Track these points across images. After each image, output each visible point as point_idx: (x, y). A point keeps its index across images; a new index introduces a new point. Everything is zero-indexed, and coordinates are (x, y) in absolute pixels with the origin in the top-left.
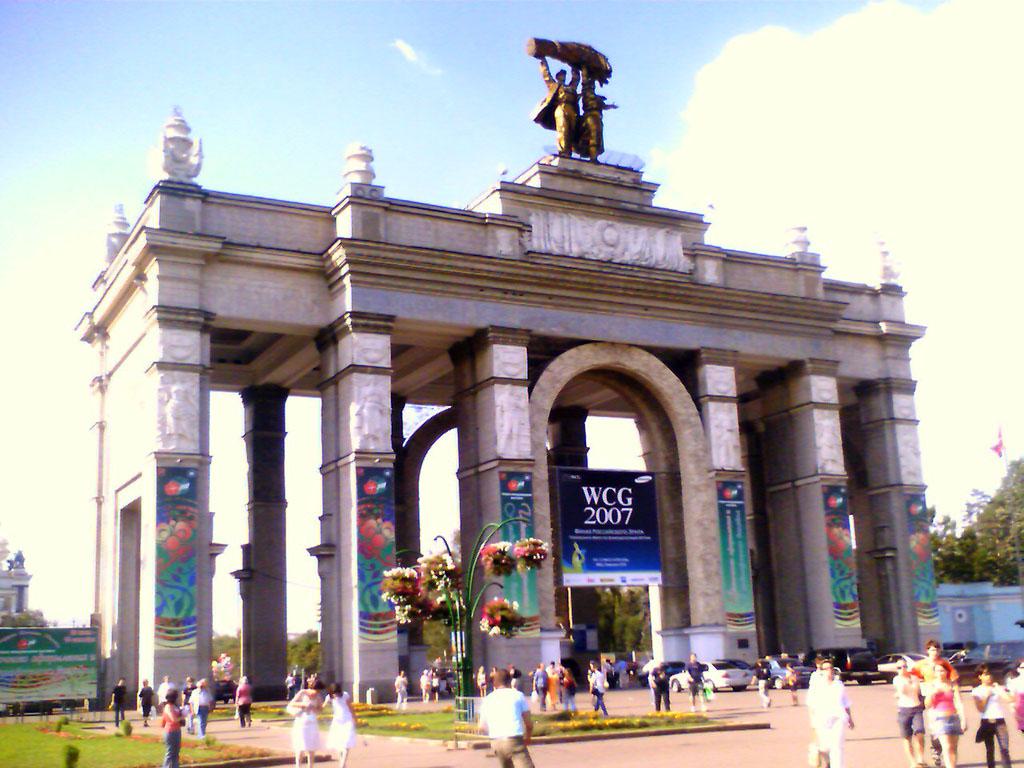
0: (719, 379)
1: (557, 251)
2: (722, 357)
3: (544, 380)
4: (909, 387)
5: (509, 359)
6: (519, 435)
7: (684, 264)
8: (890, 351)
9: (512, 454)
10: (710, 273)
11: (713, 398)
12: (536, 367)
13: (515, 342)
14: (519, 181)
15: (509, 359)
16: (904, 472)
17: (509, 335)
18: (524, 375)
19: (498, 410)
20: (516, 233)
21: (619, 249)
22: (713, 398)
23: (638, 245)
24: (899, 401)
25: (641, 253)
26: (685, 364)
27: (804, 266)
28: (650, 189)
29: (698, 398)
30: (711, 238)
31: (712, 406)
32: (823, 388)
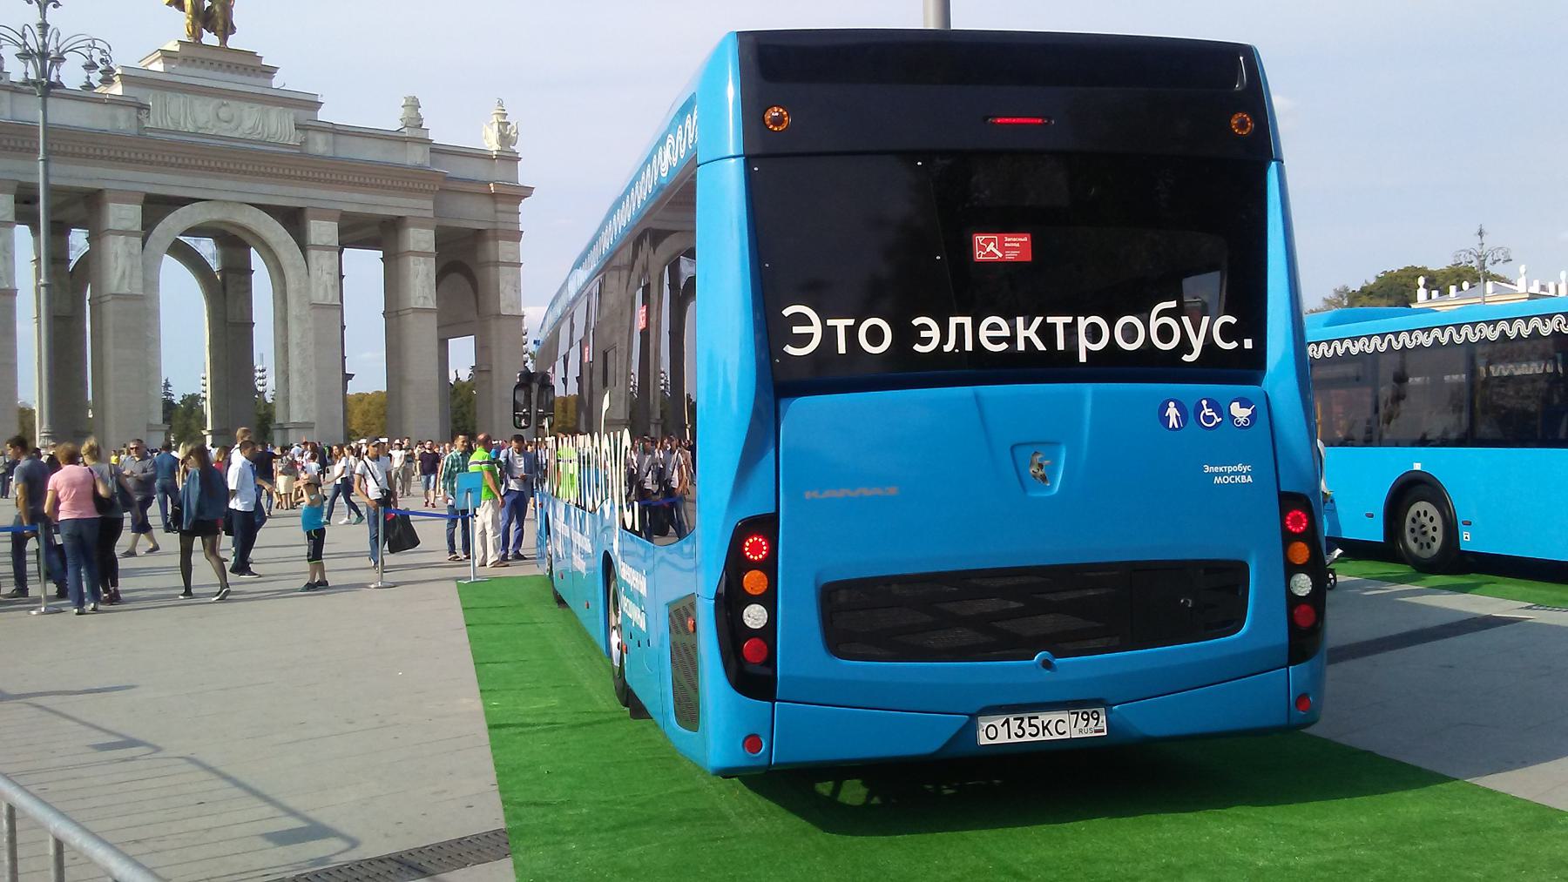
0: (322, 231)
1: (172, 128)
2: (323, 215)
3: (159, 229)
4: (516, 236)
5: (123, 215)
6: (131, 275)
7: (293, 138)
8: (500, 207)
9: (125, 290)
10: (319, 145)
11: (317, 247)
12: (148, 225)
13: (129, 202)
14: (140, 66)
15: (123, 215)
16: (502, 304)
17: (124, 197)
18: (138, 228)
19: (112, 258)
20: (134, 111)
21: (232, 125)
22: (317, 247)
23: (249, 122)
24: (504, 247)
25: (254, 128)
26: (293, 219)
27: (412, 134)
28: (270, 72)
29: (303, 247)
30: (323, 115)
31: (313, 254)
32: (420, 239)
